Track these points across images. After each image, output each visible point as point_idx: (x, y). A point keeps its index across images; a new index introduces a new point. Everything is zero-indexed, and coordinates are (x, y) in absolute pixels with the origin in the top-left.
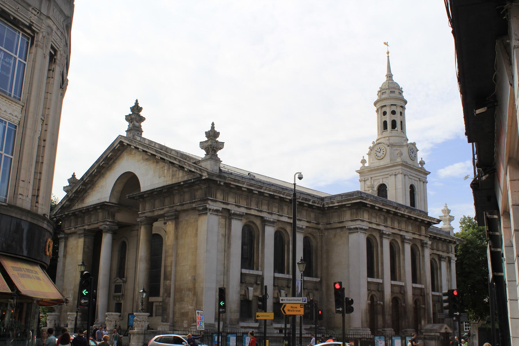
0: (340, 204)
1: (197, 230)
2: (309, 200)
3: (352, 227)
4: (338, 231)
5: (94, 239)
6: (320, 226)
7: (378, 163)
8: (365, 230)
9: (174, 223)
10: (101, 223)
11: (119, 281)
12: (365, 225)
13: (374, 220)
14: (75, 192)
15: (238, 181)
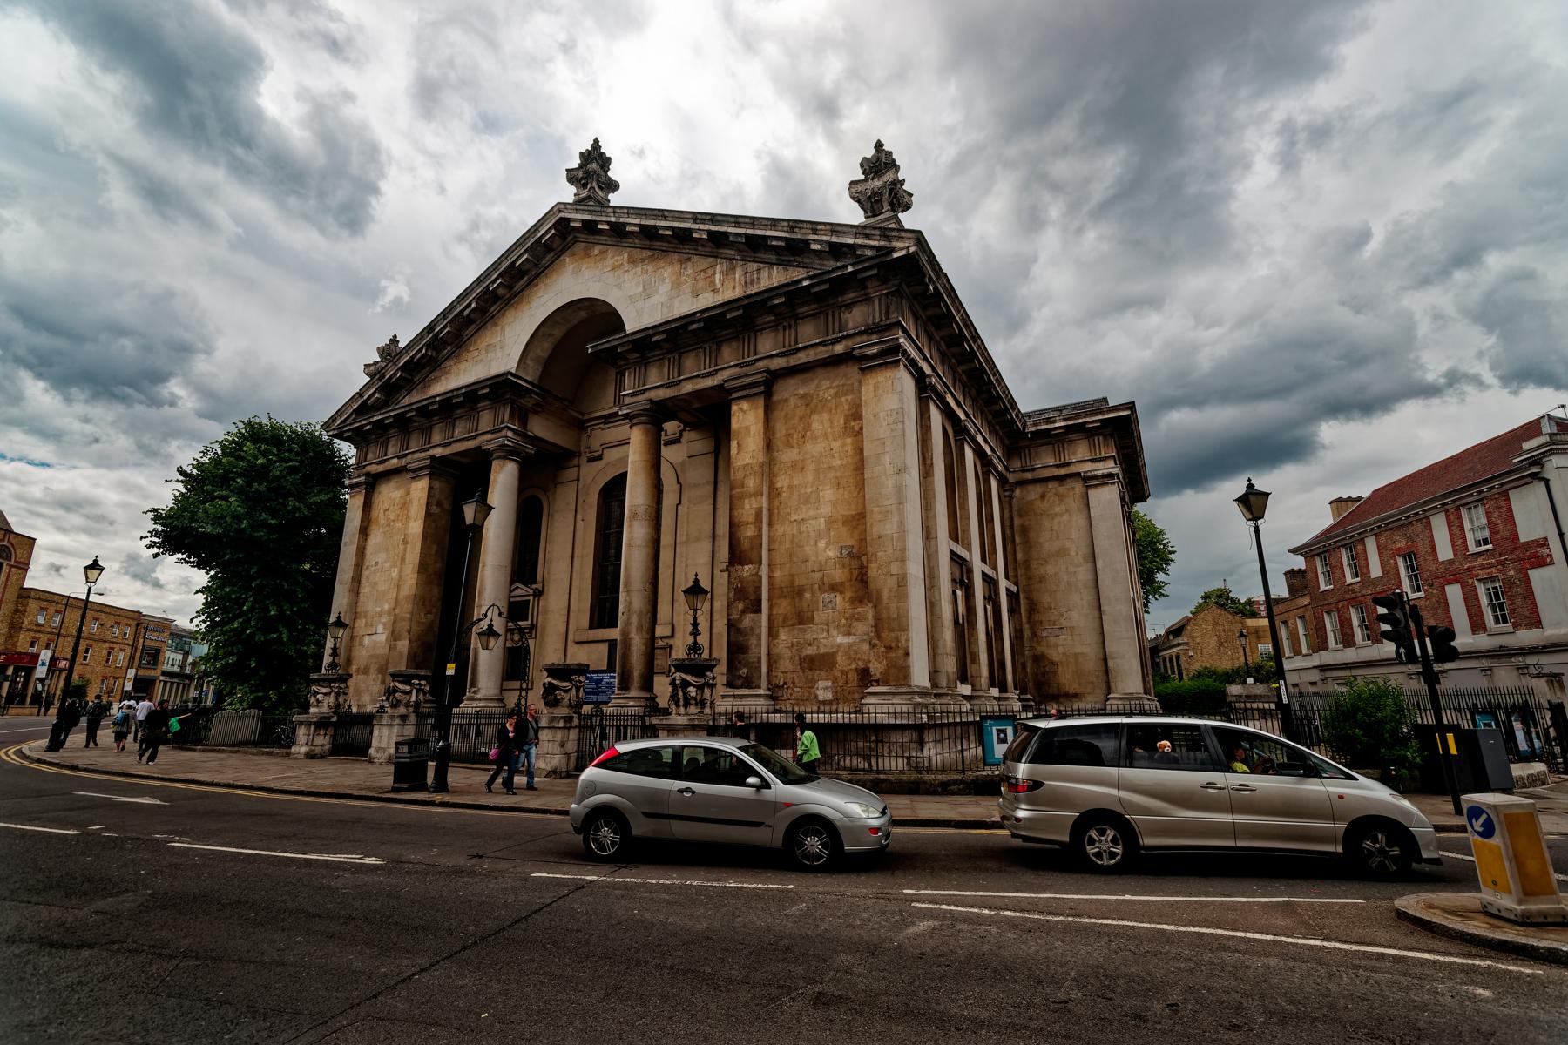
1: (856, 415)
3: (1099, 473)
5: (462, 480)
9: (761, 401)
10: (489, 436)
11: (522, 591)
14: (402, 368)
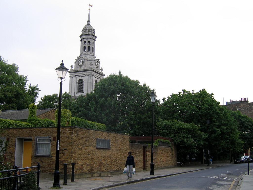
7: (79, 69)
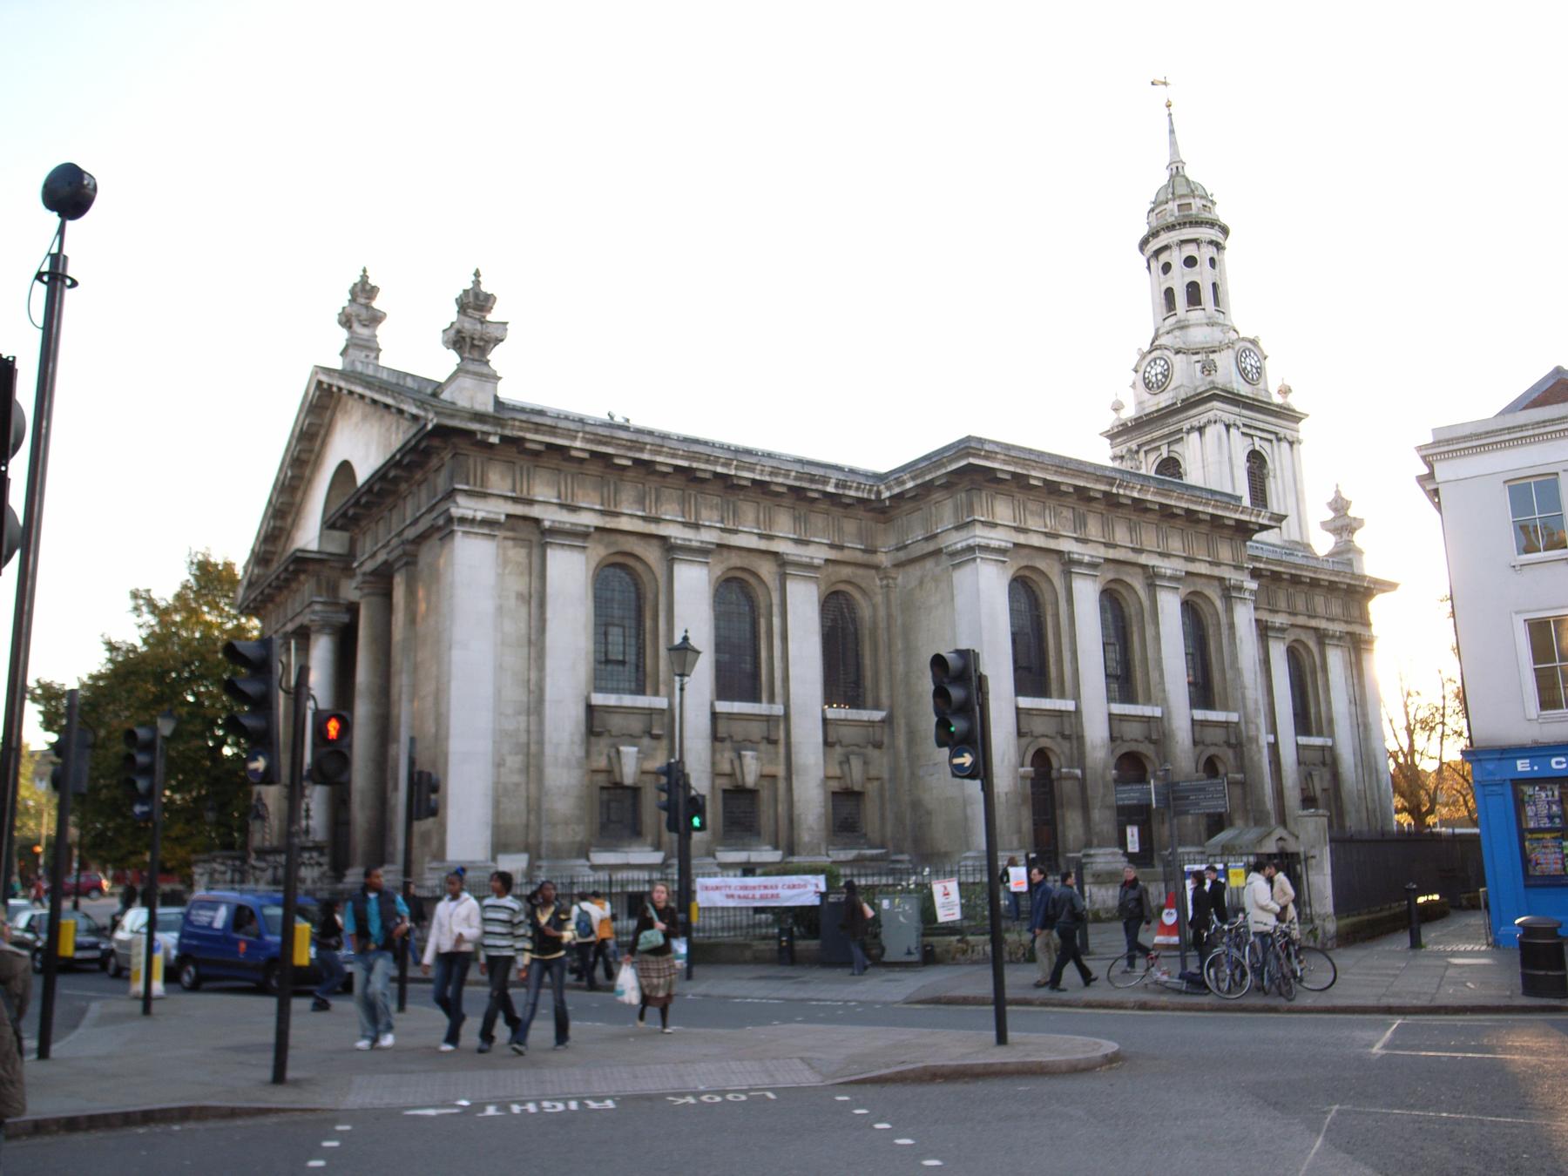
0: (919, 481)
2: (825, 480)
3: (959, 546)
4: (929, 564)
6: (883, 559)
8: (1002, 551)
12: (998, 538)
13: (1033, 523)
15: (553, 430)
